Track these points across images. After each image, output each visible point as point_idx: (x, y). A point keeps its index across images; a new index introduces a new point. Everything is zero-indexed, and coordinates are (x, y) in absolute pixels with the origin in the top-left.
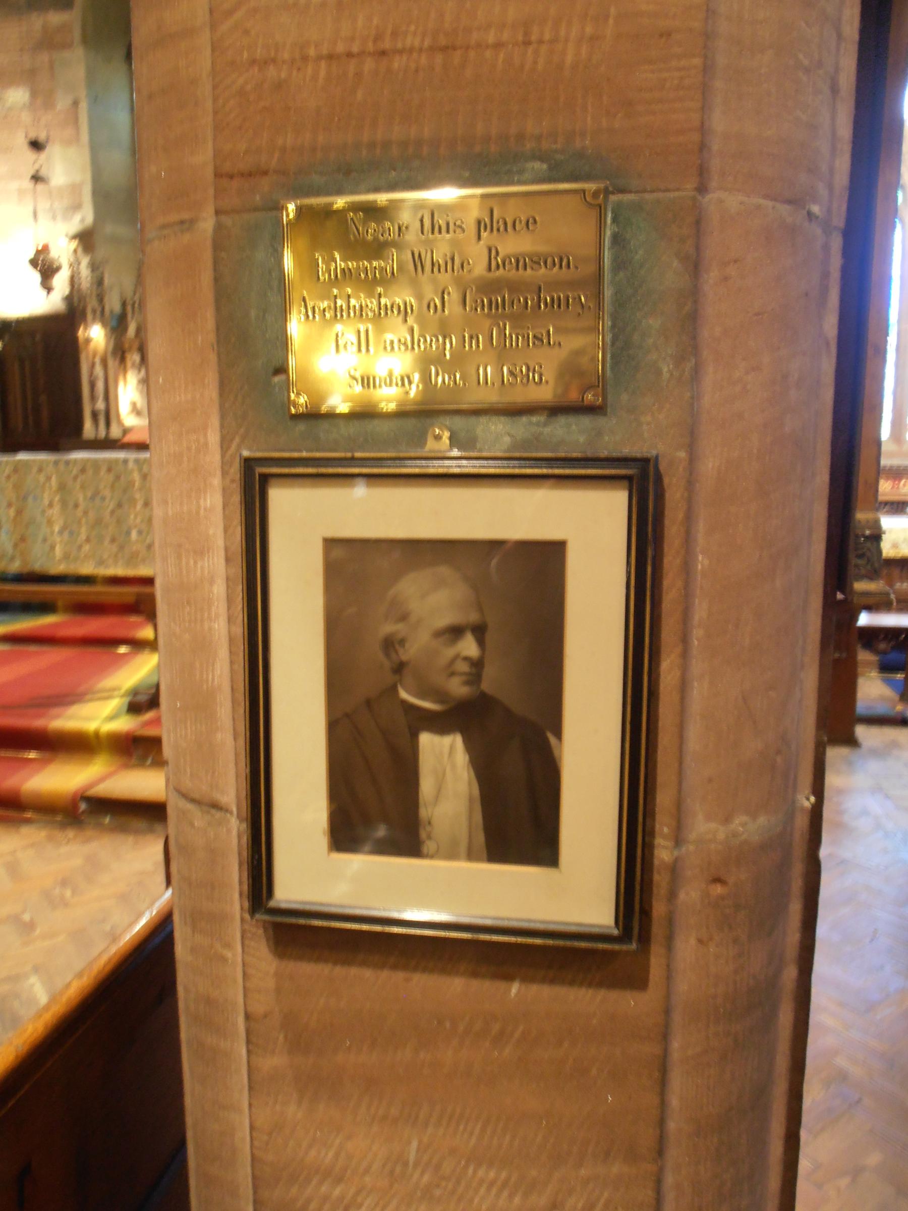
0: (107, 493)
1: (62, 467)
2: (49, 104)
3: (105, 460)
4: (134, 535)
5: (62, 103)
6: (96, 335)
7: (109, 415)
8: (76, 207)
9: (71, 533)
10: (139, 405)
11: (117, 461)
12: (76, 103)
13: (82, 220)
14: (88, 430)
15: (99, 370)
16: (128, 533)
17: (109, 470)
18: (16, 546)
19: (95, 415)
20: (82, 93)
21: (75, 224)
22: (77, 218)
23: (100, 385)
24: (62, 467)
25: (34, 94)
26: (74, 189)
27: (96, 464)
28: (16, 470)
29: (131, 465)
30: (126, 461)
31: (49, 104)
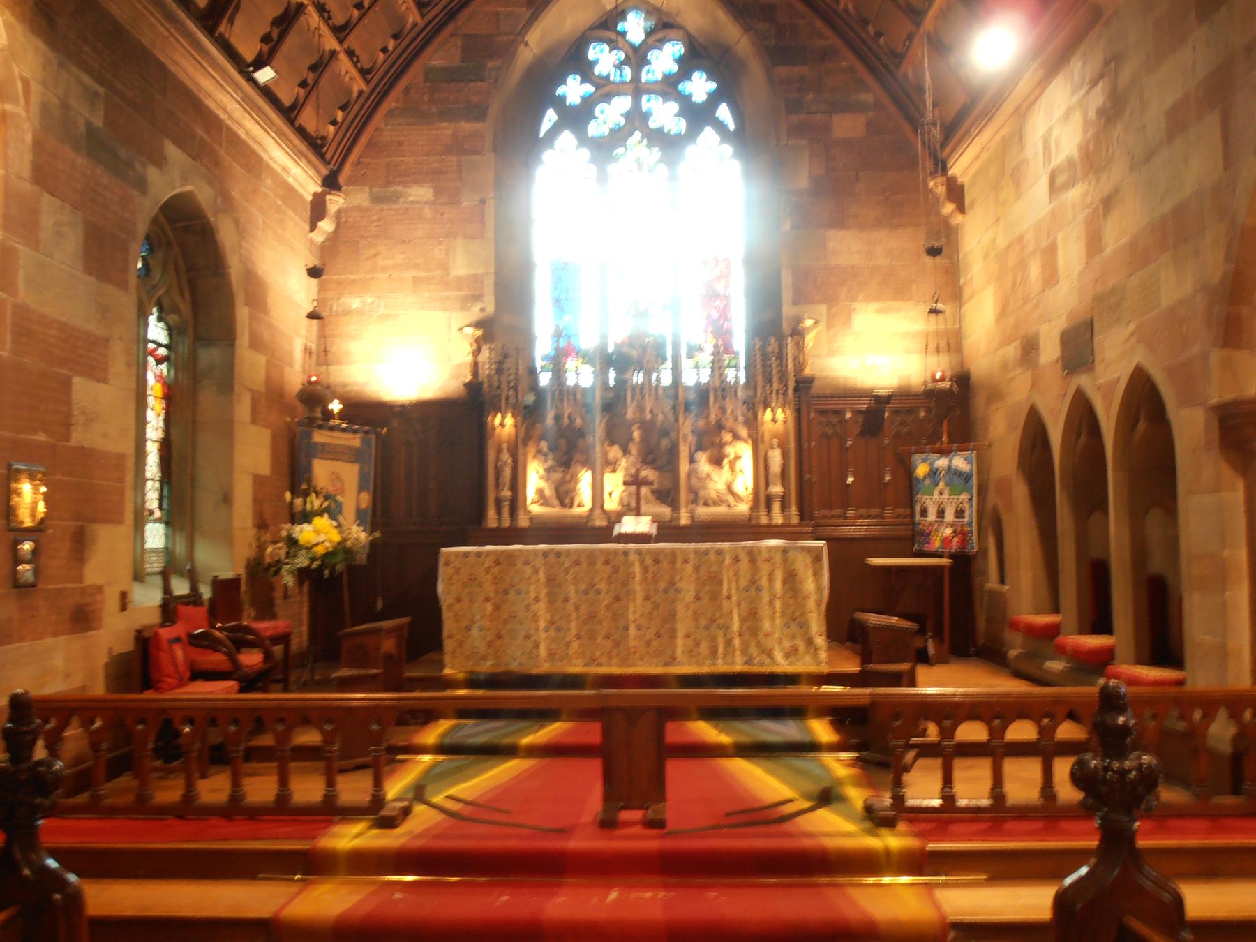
0: (603, 586)
1: (552, 558)
2: (454, 201)
3: (601, 550)
4: (632, 631)
6: (504, 424)
7: (516, 502)
8: (477, 298)
9: (559, 630)
10: (548, 492)
11: (615, 552)
12: (483, 202)
13: (482, 310)
14: (491, 520)
15: (506, 457)
16: (626, 628)
17: (607, 562)
18: (490, 644)
19: (498, 502)
21: (475, 313)
22: (477, 308)
23: (507, 472)
24: (552, 558)
25: (438, 192)
26: (476, 280)
27: (592, 556)
28: (497, 563)
29: (632, 557)
30: (626, 553)
31: (454, 201)
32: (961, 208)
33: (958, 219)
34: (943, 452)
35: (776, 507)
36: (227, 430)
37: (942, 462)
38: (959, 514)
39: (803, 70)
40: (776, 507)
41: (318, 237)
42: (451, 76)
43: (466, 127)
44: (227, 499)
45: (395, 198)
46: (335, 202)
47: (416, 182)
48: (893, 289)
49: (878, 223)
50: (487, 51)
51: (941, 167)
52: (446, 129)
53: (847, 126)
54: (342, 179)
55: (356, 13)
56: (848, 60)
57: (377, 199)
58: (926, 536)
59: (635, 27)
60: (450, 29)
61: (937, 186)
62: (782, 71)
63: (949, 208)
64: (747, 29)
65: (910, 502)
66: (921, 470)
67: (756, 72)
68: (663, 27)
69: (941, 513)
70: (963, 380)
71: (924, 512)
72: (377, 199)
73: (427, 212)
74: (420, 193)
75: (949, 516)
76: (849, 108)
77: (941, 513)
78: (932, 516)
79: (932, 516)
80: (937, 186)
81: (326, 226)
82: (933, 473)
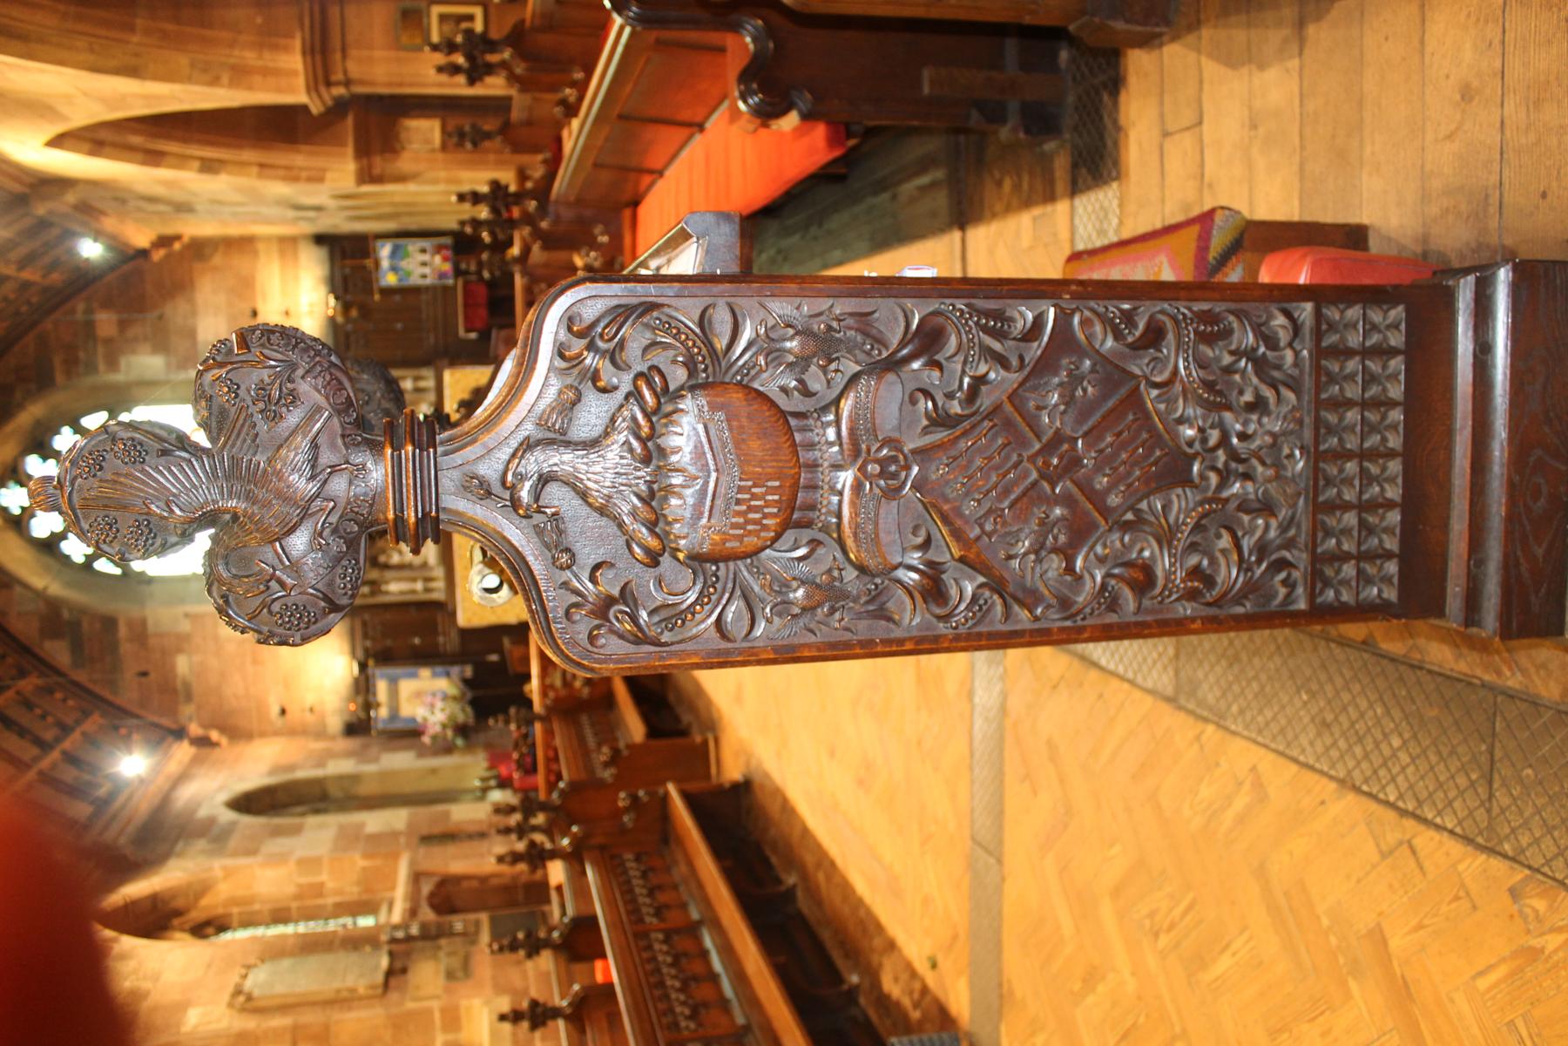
5: (185, 626)
12: (187, 615)
14: (439, 595)
20: (180, 610)
25: (180, 650)
32: (178, 237)
33: (186, 239)
34: (377, 264)
35: (422, 384)
36: (384, 775)
37: (385, 264)
38: (423, 251)
39: (57, 361)
40: (422, 384)
41: (224, 741)
42: (77, 647)
43: (123, 631)
44: (434, 771)
45: (187, 687)
46: (195, 729)
47: (173, 667)
48: (246, 286)
49: (191, 301)
50: (56, 619)
51: (143, 253)
52: (126, 648)
53: (106, 322)
54: (174, 726)
55: (50, 719)
56: (48, 324)
57: (189, 697)
58: (442, 275)
59: (14, 498)
60: (37, 651)
61: (158, 255)
62: (60, 377)
63: (177, 246)
64: (21, 406)
65: (416, 290)
66: (391, 279)
67: (58, 399)
68: (13, 474)
69: (424, 264)
70: (320, 239)
71: (424, 276)
72: (189, 697)
73: (196, 658)
74: (182, 665)
75: (426, 257)
76: (90, 326)
77: (424, 264)
78: (427, 270)
79: (427, 270)
80: (158, 255)
81: (214, 735)
82: (394, 269)
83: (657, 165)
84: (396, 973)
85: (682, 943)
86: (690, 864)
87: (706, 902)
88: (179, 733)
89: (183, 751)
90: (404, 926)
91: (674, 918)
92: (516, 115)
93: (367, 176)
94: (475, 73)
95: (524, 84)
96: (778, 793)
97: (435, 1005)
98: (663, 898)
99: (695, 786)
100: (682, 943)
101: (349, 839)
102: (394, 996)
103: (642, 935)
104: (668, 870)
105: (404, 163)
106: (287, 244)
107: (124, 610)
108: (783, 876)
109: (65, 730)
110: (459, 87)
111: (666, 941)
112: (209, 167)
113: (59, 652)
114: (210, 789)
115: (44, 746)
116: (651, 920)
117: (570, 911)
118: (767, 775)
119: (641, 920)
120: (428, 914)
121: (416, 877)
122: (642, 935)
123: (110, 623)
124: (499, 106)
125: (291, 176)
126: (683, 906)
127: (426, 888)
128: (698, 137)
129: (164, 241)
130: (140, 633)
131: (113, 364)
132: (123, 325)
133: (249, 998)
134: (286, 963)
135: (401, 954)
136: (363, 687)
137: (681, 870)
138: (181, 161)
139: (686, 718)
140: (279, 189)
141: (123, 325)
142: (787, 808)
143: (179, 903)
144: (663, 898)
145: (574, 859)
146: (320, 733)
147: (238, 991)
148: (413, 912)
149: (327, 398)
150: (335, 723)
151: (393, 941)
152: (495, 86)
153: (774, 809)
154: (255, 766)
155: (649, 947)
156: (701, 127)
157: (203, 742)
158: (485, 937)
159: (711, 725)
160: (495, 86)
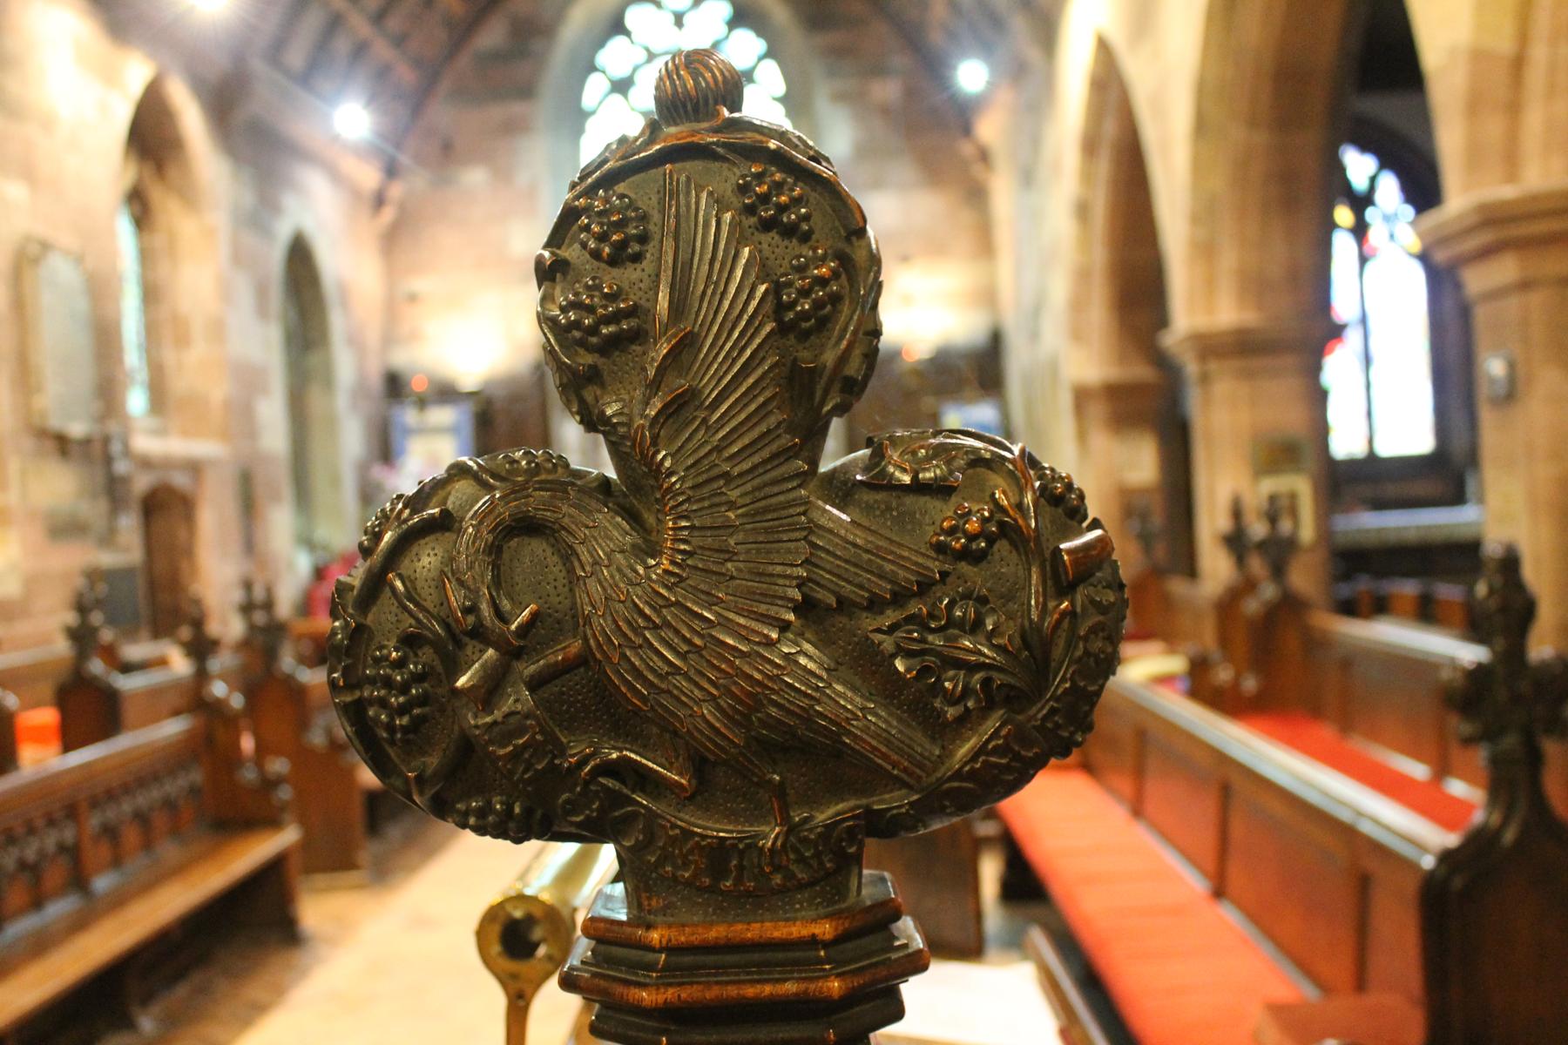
36: (332, 423)
42: (499, 57)
44: (335, 481)
46: (396, 191)
48: (935, 248)
53: (888, 90)
81: (388, 214)
83: (1150, 807)
84: (62, 445)
85: (55, 875)
86: (177, 871)
87: (118, 901)
88: (391, 171)
89: (369, 176)
90: (127, 452)
91: (97, 853)
92: (1178, 587)
93: (1082, 396)
94: (1236, 541)
95: (1227, 605)
96: (279, 992)
97: (12, 497)
98: (131, 836)
99: (295, 863)
100: (55, 875)
101: (249, 381)
102: (28, 443)
103: (72, 812)
104: (175, 831)
105: (1101, 441)
106: (988, 297)
107: (543, 108)
108: (156, 1009)
109: (399, 41)
110: (1211, 521)
111: (62, 848)
112: (1082, 211)
113: (492, 36)
114: (320, 210)
115: (379, 18)
116: (94, 821)
117: (127, 684)
118: (303, 973)
119: (95, 803)
120: (142, 483)
121: (195, 468)
122: (72, 812)
123: (526, 91)
124: (1188, 565)
125: (1077, 305)
126: (116, 862)
127: (180, 480)
128: (1195, 883)
129: (984, 156)
130: (513, 128)
131: (840, 97)
132: (885, 111)
133: (36, 261)
134: (82, 305)
135: (92, 453)
136: (446, 393)
137: (169, 851)
138: (1087, 176)
139: (394, 832)
140: (1059, 289)
141: (885, 111)
142: (258, 1010)
143: (172, 172)
144: (131, 836)
145: (194, 699)
146: (389, 338)
147: (46, 246)
148: (146, 463)
149: (958, 775)
150: (401, 358)
151: (106, 441)
152: (1216, 567)
153: (254, 990)
154: (348, 262)
155: (51, 822)
156: (1219, 893)
157: (379, 201)
158: (107, 559)
159: (383, 874)
160: (1216, 567)
